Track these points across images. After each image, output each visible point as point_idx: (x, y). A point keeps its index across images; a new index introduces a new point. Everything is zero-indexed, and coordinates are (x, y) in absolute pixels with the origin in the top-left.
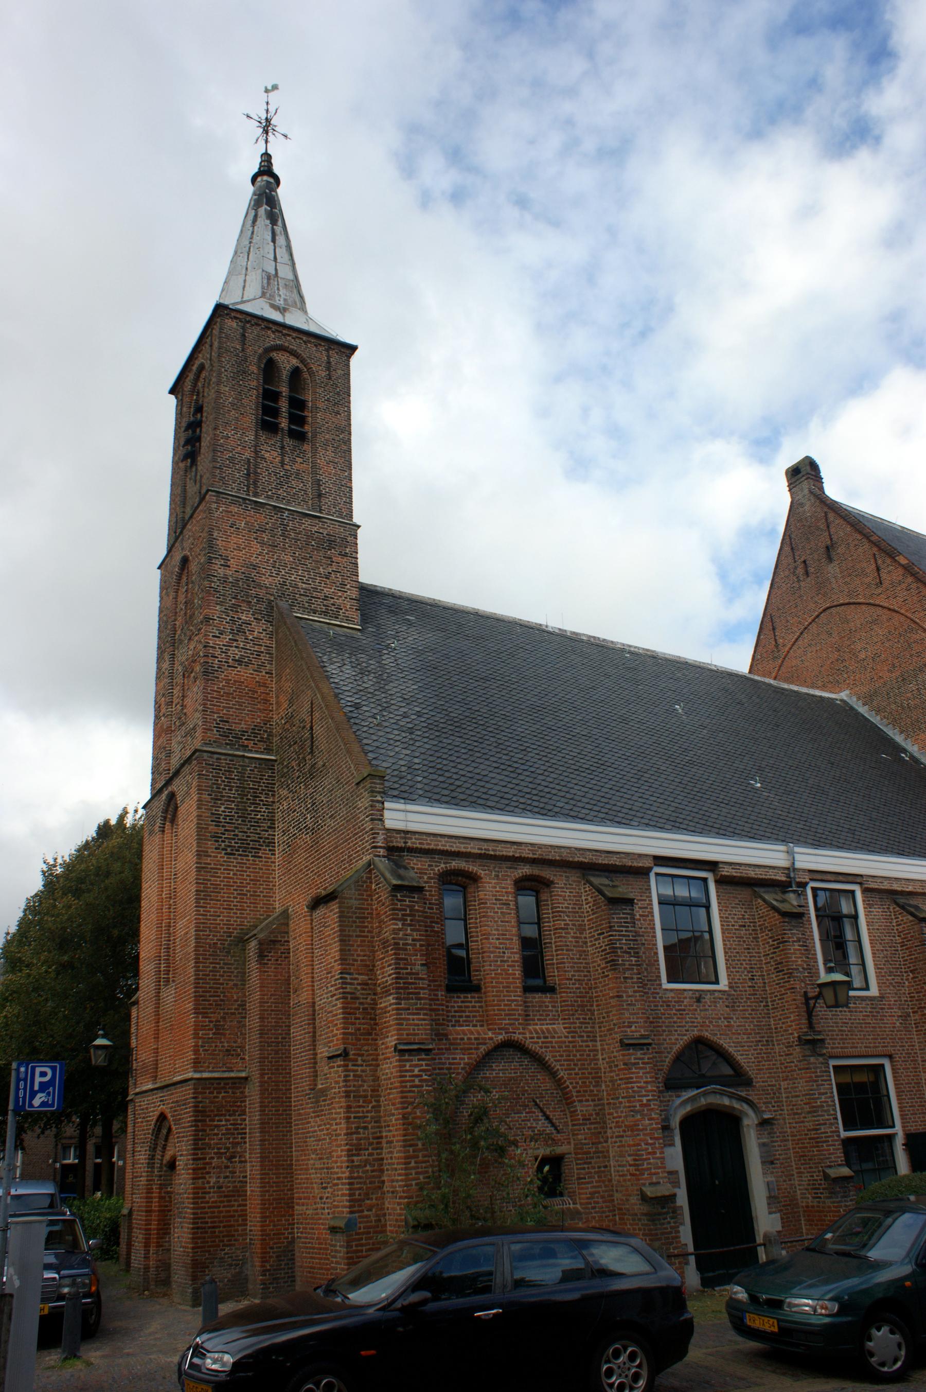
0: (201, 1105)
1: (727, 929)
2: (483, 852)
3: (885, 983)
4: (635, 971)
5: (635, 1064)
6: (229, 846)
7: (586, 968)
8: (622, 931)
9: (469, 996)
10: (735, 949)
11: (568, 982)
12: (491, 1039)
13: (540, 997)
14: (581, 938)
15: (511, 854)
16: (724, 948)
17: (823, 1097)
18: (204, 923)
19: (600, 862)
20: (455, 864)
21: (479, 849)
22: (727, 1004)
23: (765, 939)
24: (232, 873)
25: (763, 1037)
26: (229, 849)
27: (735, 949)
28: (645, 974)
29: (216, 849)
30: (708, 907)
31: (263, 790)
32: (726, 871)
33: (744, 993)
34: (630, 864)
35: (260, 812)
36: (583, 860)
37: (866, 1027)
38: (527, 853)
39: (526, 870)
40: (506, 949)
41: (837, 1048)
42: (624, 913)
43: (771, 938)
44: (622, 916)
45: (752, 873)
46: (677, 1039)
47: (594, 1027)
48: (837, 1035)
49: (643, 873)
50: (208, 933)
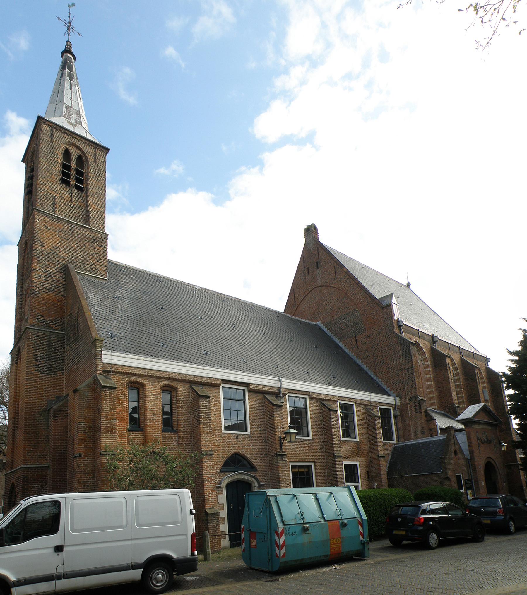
0: (26, 478)
1: (251, 410)
2: (146, 374)
4: (209, 425)
5: (206, 462)
6: (42, 370)
7: (190, 423)
8: (204, 409)
9: (138, 433)
10: (254, 418)
11: (181, 429)
13: (170, 434)
14: (188, 411)
15: (159, 376)
16: (250, 418)
18: (29, 402)
19: (198, 380)
20: (134, 379)
21: (144, 373)
22: (249, 440)
23: (267, 415)
24: (43, 381)
25: (263, 453)
26: (42, 371)
27: (254, 418)
29: (36, 371)
30: (244, 401)
31: (59, 346)
32: (252, 387)
33: (256, 436)
34: (211, 382)
35: (58, 356)
36: (191, 379)
37: (305, 451)
38: (165, 375)
39: (166, 383)
40: (155, 414)
41: (293, 458)
42: (205, 402)
43: (269, 414)
44: (204, 402)
46: (227, 453)
47: (191, 447)
48: (294, 453)
49: (218, 386)
50: (31, 406)
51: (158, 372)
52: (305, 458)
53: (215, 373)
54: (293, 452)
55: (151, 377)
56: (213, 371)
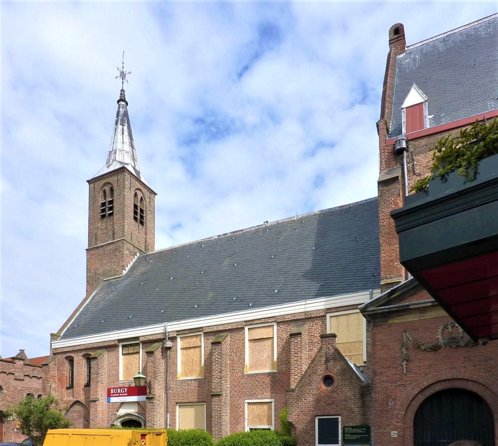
3: (209, 372)
12: (73, 400)
15: (79, 349)
17: (150, 417)
28: (114, 379)
34: (110, 344)
37: (194, 391)
38: (82, 347)
45: (151, 338)
51: (78, 346)
52: (193, 399)
53: (111, 336)
54: (180, 393)
55: (75, 351)
56: (110, 335)
